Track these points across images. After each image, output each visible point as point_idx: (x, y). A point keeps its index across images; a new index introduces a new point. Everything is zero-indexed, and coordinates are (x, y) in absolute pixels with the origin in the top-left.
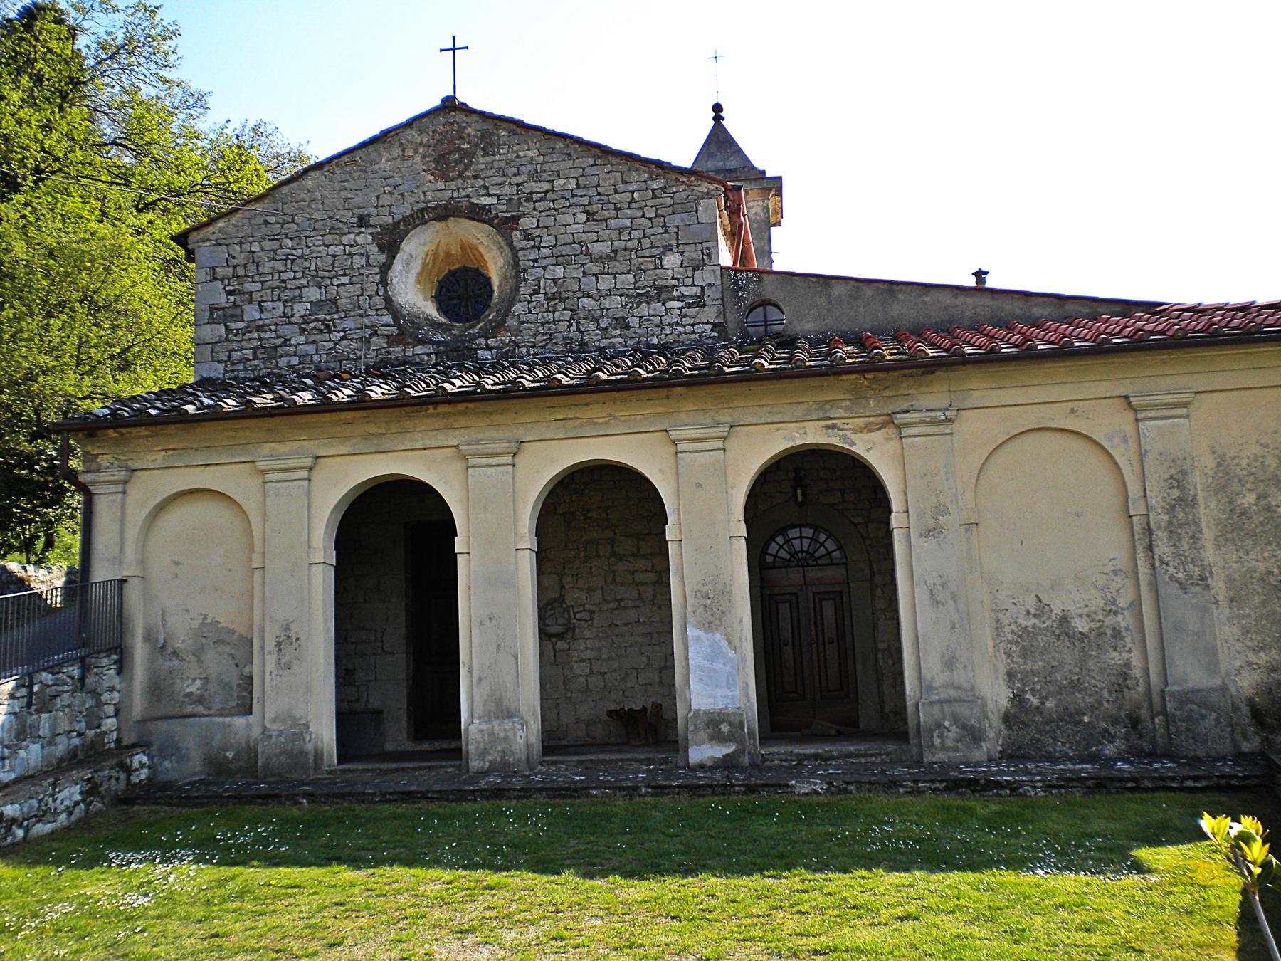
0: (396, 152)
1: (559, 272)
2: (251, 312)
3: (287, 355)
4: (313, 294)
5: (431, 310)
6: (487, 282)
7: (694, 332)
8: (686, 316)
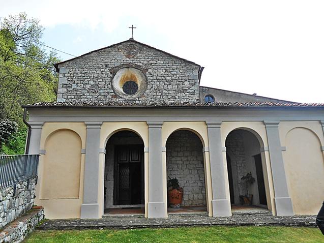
0: (117, 50)
2: (74, 86)
3: (83, 98)
4: (92, 83)
5: (122, 90)
6: (137, 84)
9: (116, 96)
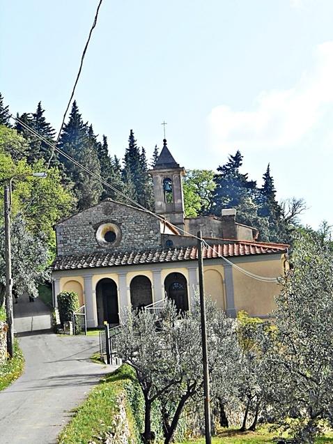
1: (130, 234)
2: (69, 242)
4: (81, 238)
9: (99, 247)
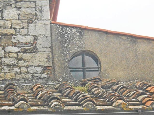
7: (28, 73)
8: (21, 59)
